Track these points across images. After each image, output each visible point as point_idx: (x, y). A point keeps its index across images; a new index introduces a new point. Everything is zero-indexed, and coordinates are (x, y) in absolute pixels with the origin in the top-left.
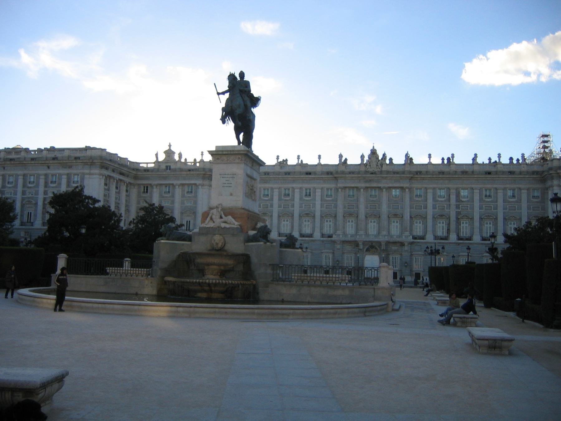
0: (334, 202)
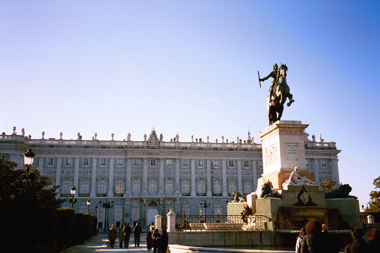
0: (124, 169)
